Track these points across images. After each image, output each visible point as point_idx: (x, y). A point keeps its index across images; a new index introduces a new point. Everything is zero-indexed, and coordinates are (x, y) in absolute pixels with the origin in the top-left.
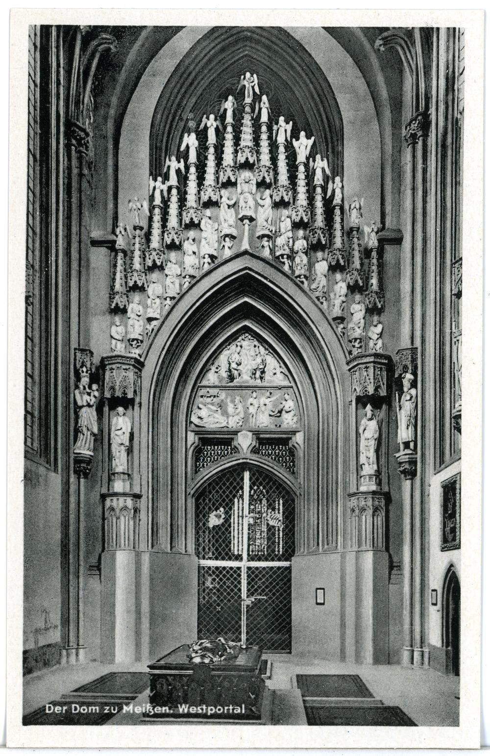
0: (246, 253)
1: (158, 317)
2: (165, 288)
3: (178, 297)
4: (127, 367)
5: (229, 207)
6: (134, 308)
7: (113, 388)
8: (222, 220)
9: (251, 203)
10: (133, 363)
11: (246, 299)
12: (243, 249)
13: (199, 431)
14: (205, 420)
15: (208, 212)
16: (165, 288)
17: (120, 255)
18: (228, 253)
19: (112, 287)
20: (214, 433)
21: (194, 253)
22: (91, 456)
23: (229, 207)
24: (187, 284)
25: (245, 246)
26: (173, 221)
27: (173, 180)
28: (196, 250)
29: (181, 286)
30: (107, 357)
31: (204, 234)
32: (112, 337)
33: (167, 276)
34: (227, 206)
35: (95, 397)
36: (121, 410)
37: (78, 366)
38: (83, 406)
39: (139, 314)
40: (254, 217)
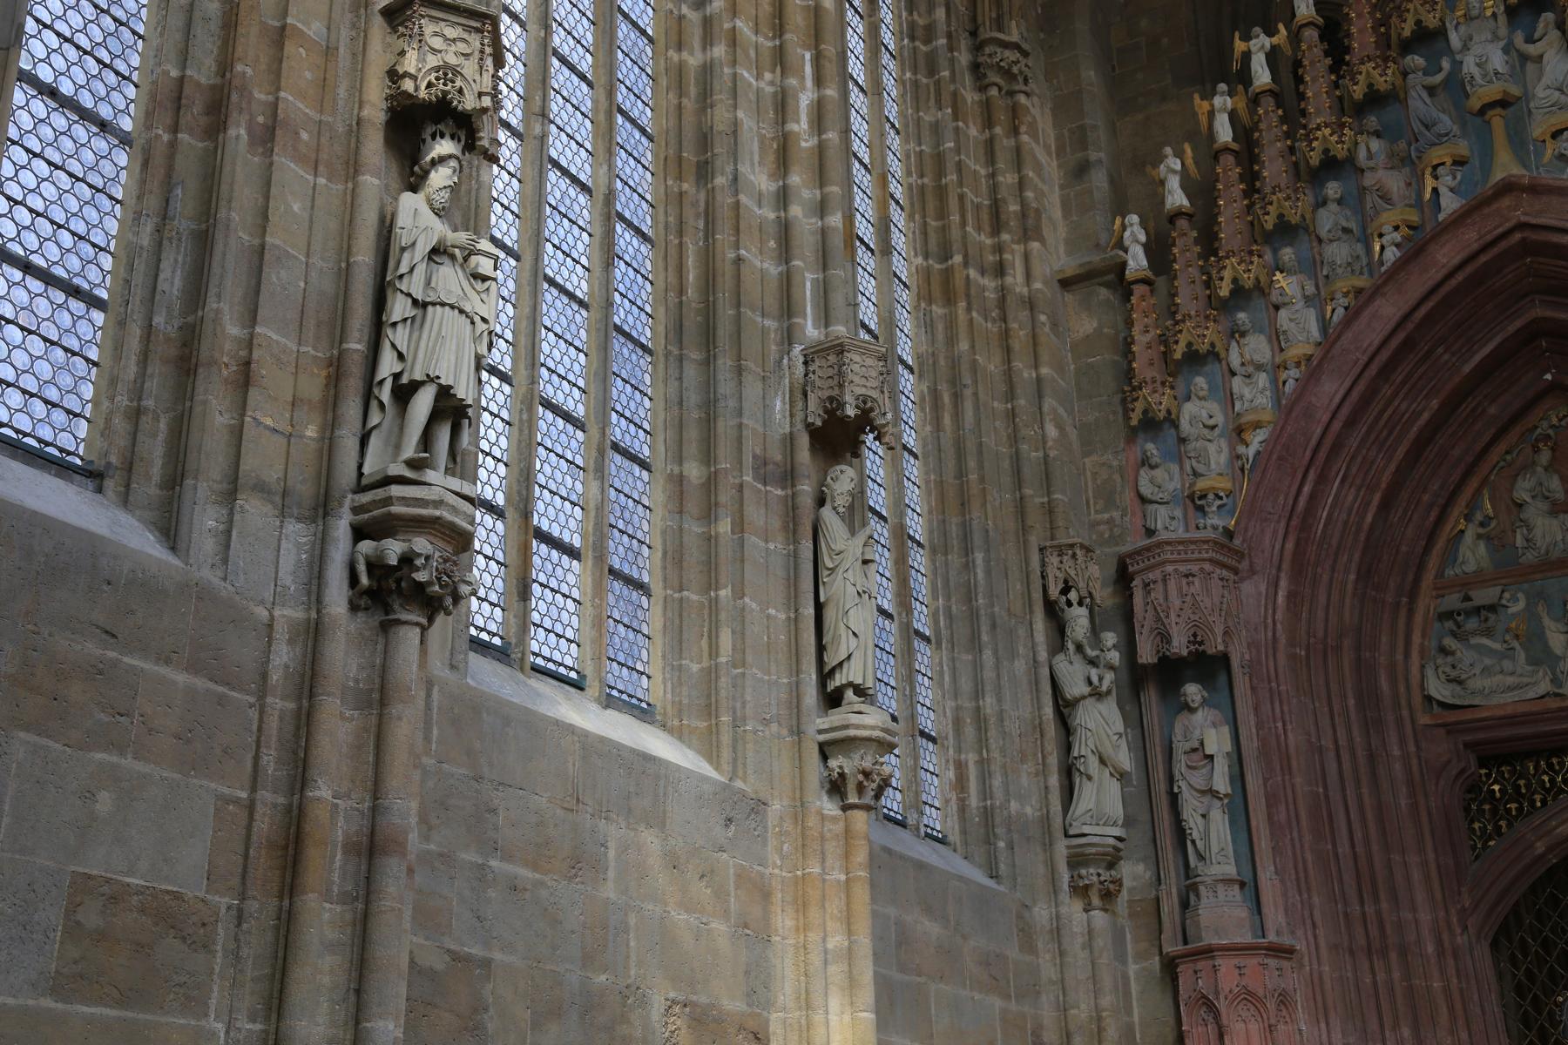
0: (1508, 187)
1: (1266, 416)
2: (1277, 338)
3: (1318, 353)
4: (1194, 568)
5: (1431, 90)
6: (1198, 411)
7: (1165, 637)
8: (1417, 126)
9: (1497, 61)
10: (1211, 554)
11: (1540, 312)
12: (1498, 175)
13: (1453, 720)
14: (1471, 684)
15: (1372, 121)
16: (1277, 338)
17: (1139, 290)
18: (1450, 204)
19: (1129, 374)
20: (1511, 720)
21: (1346, 230)
22: (1119, 839)
23: (1431, 90)
24: (1340, 311)
25: (1506, 166)
26: (1273, 169)
27: (1262, 76)
28: (1353, 225)
29: (1324, 325)
30: (1131, 555)
31: (1369, 180)
32: (1144, 500)
33: (1277, 308)
34: (1425, 95)
35: (1112, 668)
36: (1193, 691)
37: (1054, 592)
38: (1077, 701)
39: (1211, 422)
40: (1515, 90)
